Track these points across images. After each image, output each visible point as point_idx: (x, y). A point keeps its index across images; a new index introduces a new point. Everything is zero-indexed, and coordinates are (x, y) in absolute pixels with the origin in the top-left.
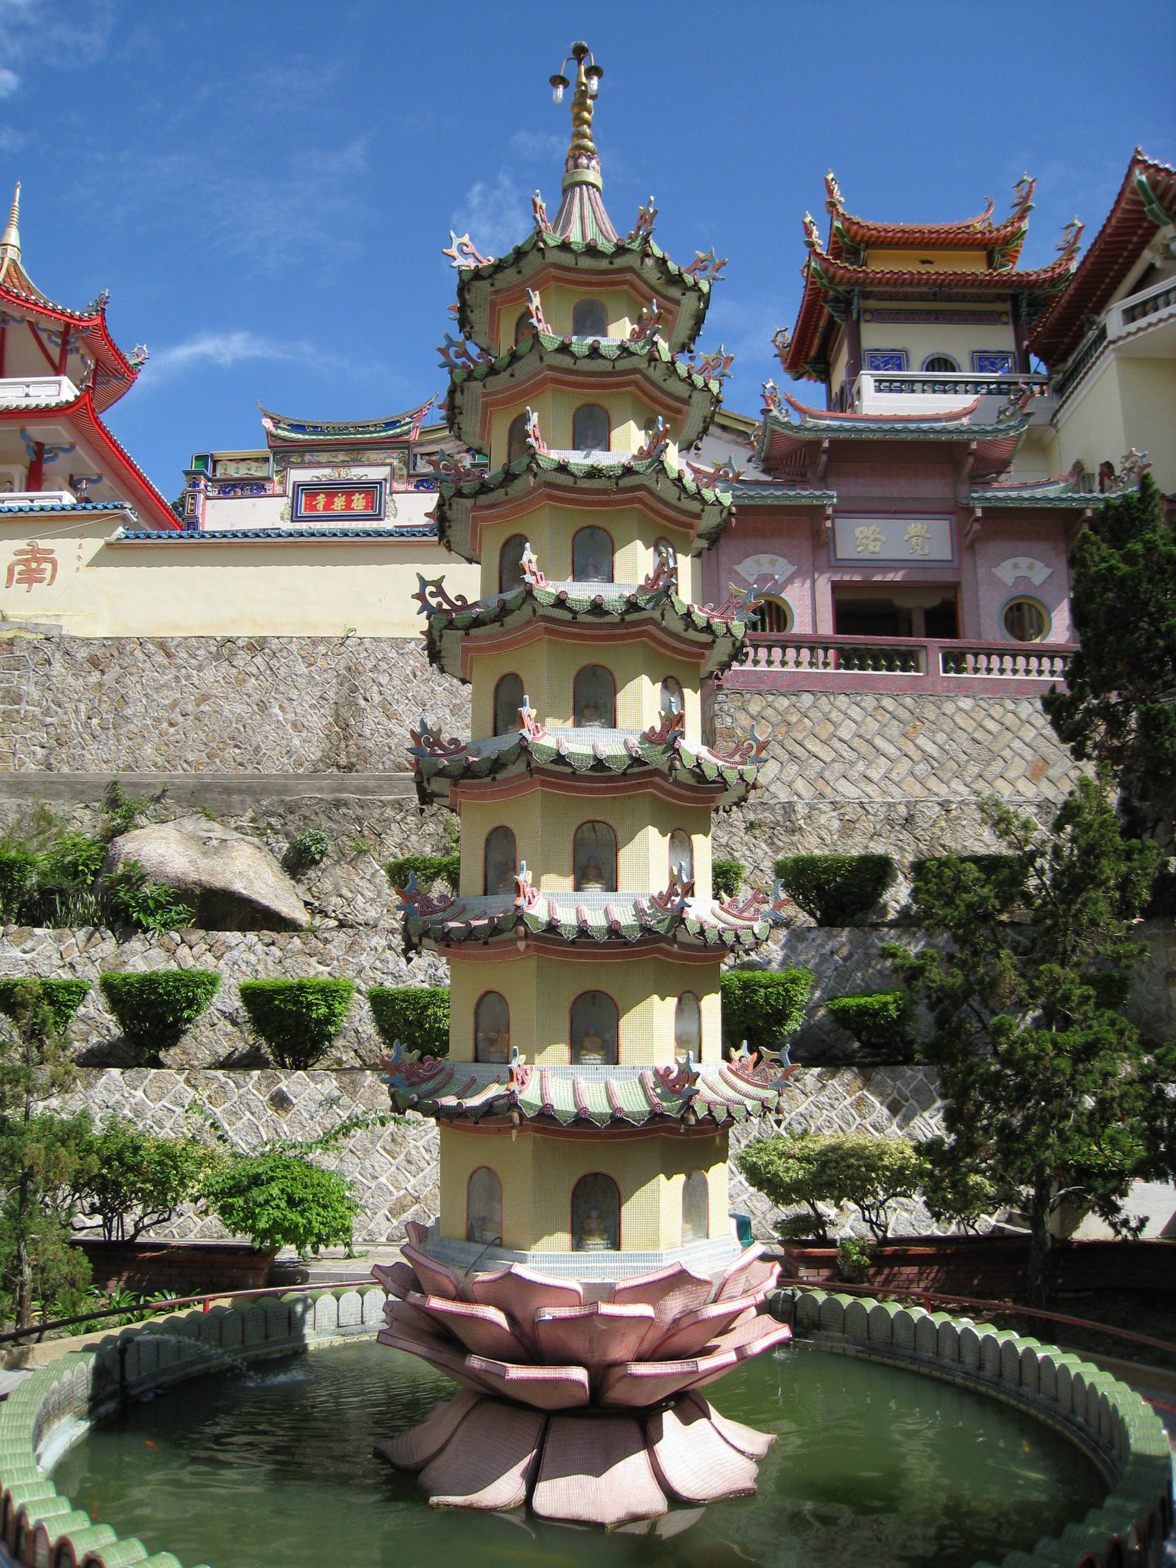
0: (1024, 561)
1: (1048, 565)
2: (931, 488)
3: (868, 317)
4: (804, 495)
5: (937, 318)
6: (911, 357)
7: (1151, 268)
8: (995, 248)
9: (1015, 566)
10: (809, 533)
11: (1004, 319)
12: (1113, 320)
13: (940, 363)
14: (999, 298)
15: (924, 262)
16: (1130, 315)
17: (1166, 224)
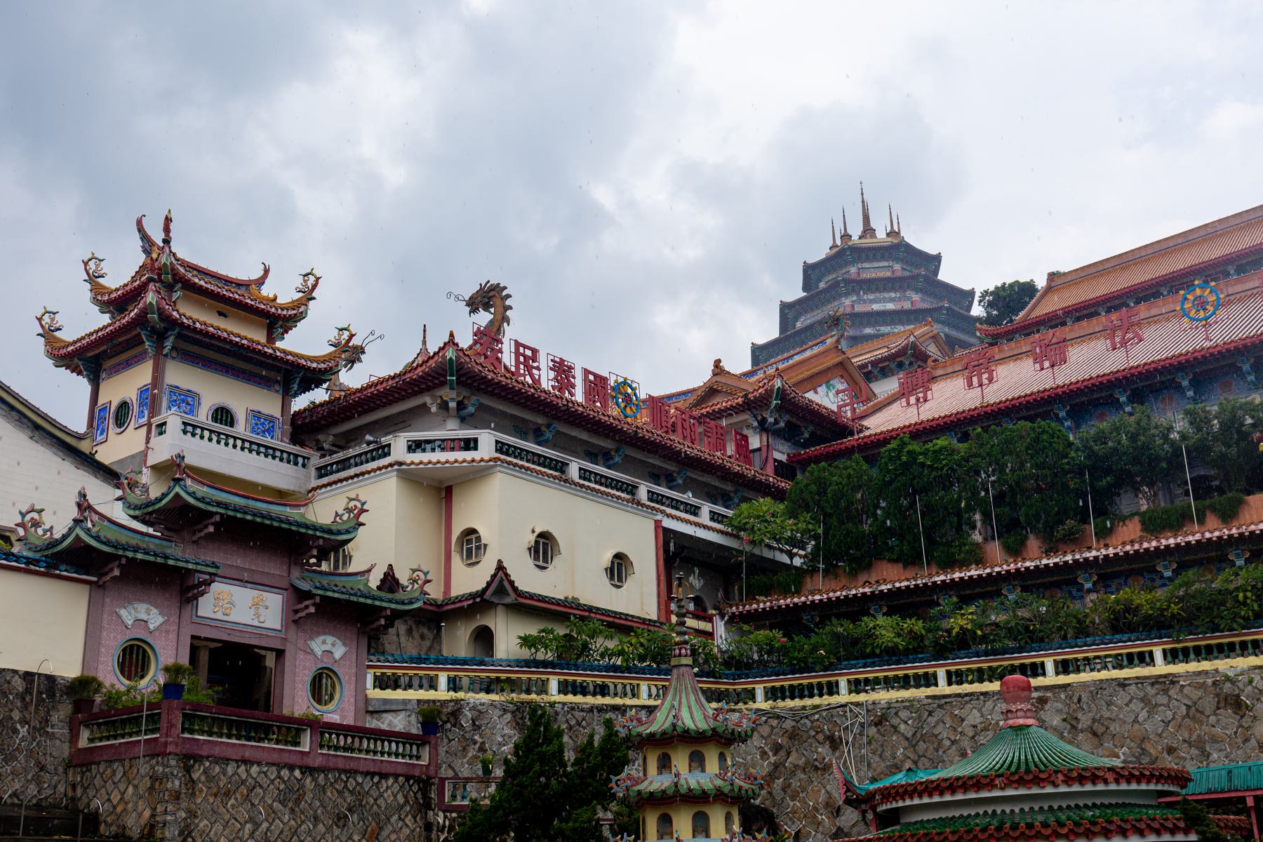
0: (330, 639)
1: (344, 644)
2: (273, 568)
3: (174, 355)
4: (180, 554)
5: (227, 372)
6: (203, 401)
7: (424, 408)
8: (279, 320)
9: (324, 642)
10: (181, 587)
11: (277, 387)
12: (399, 445)
13: (223, 415)
14: (278, 370)
15: (220, 314)
16: (415, 446)
17: (452, 388)
